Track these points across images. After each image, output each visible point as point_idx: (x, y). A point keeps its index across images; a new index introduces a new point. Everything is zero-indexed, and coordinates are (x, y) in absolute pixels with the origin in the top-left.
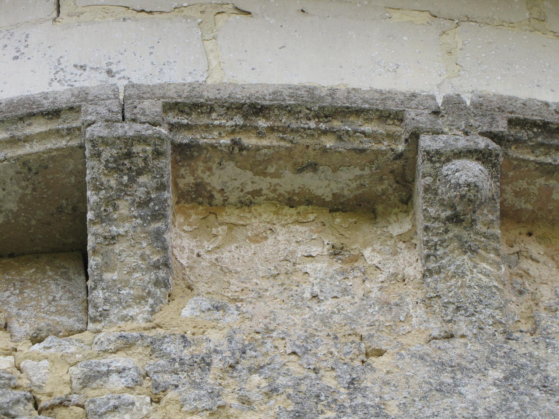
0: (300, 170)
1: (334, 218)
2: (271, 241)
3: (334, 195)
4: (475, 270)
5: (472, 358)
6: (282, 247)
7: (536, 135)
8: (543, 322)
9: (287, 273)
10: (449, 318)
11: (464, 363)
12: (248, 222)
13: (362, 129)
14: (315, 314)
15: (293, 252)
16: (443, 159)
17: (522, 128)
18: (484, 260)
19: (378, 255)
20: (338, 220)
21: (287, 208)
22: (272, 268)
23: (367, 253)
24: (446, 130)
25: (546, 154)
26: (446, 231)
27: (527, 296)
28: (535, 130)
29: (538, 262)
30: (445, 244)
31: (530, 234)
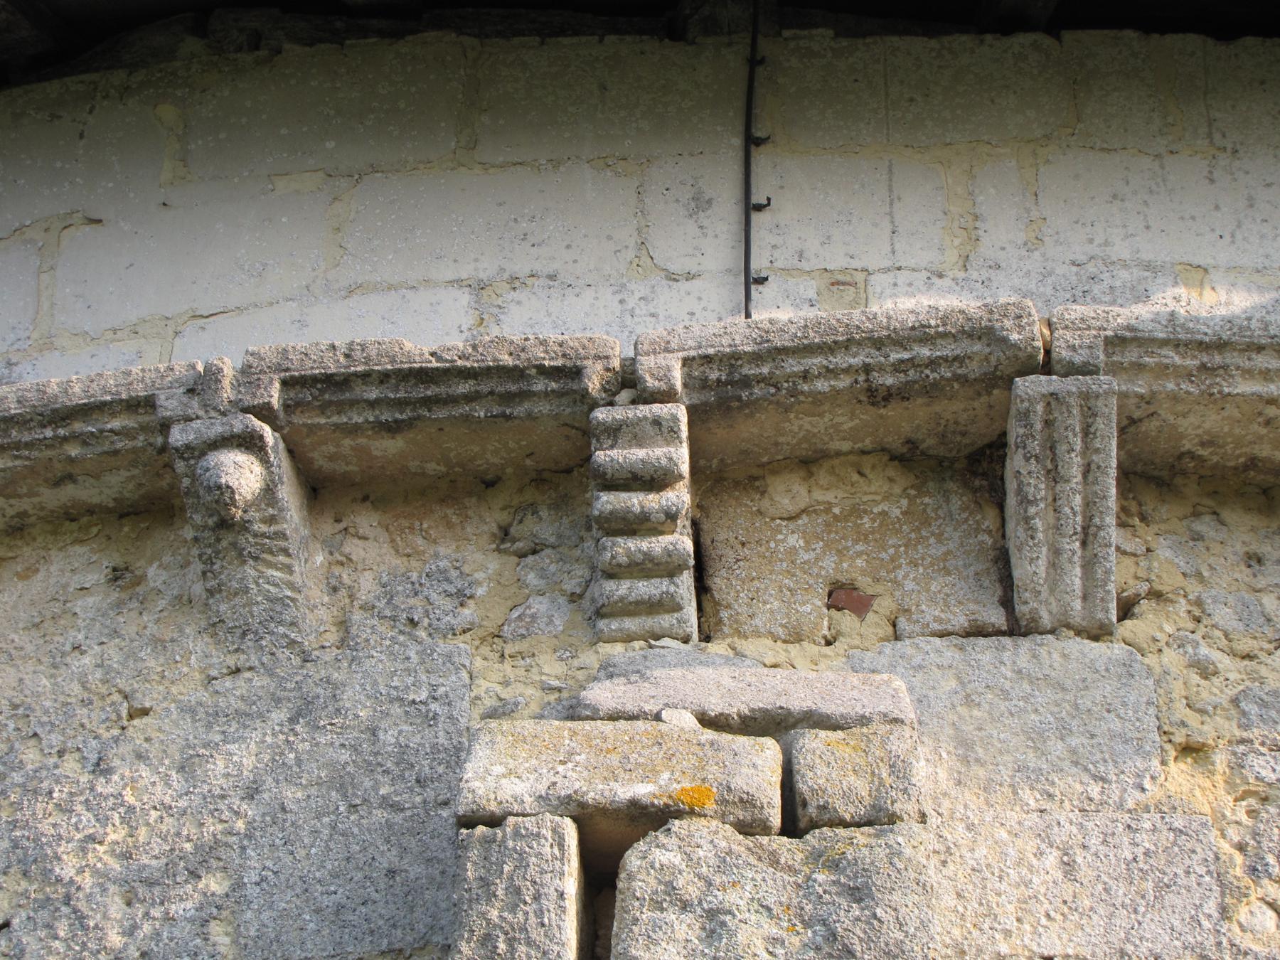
0: (58, 483)
1: (122, 526)
3: (115, 499)
6: (52, 581)
7: (322, 391)
13: (109, 426)
15: (65, 587)
16: (196, 453)
19: (164, 573)
21: (67, 523)
23: (151, 571)
25: (339, 413)
26: (219, 540)
28: (319, 386)
29: (366, 539)
30: (221, 556)
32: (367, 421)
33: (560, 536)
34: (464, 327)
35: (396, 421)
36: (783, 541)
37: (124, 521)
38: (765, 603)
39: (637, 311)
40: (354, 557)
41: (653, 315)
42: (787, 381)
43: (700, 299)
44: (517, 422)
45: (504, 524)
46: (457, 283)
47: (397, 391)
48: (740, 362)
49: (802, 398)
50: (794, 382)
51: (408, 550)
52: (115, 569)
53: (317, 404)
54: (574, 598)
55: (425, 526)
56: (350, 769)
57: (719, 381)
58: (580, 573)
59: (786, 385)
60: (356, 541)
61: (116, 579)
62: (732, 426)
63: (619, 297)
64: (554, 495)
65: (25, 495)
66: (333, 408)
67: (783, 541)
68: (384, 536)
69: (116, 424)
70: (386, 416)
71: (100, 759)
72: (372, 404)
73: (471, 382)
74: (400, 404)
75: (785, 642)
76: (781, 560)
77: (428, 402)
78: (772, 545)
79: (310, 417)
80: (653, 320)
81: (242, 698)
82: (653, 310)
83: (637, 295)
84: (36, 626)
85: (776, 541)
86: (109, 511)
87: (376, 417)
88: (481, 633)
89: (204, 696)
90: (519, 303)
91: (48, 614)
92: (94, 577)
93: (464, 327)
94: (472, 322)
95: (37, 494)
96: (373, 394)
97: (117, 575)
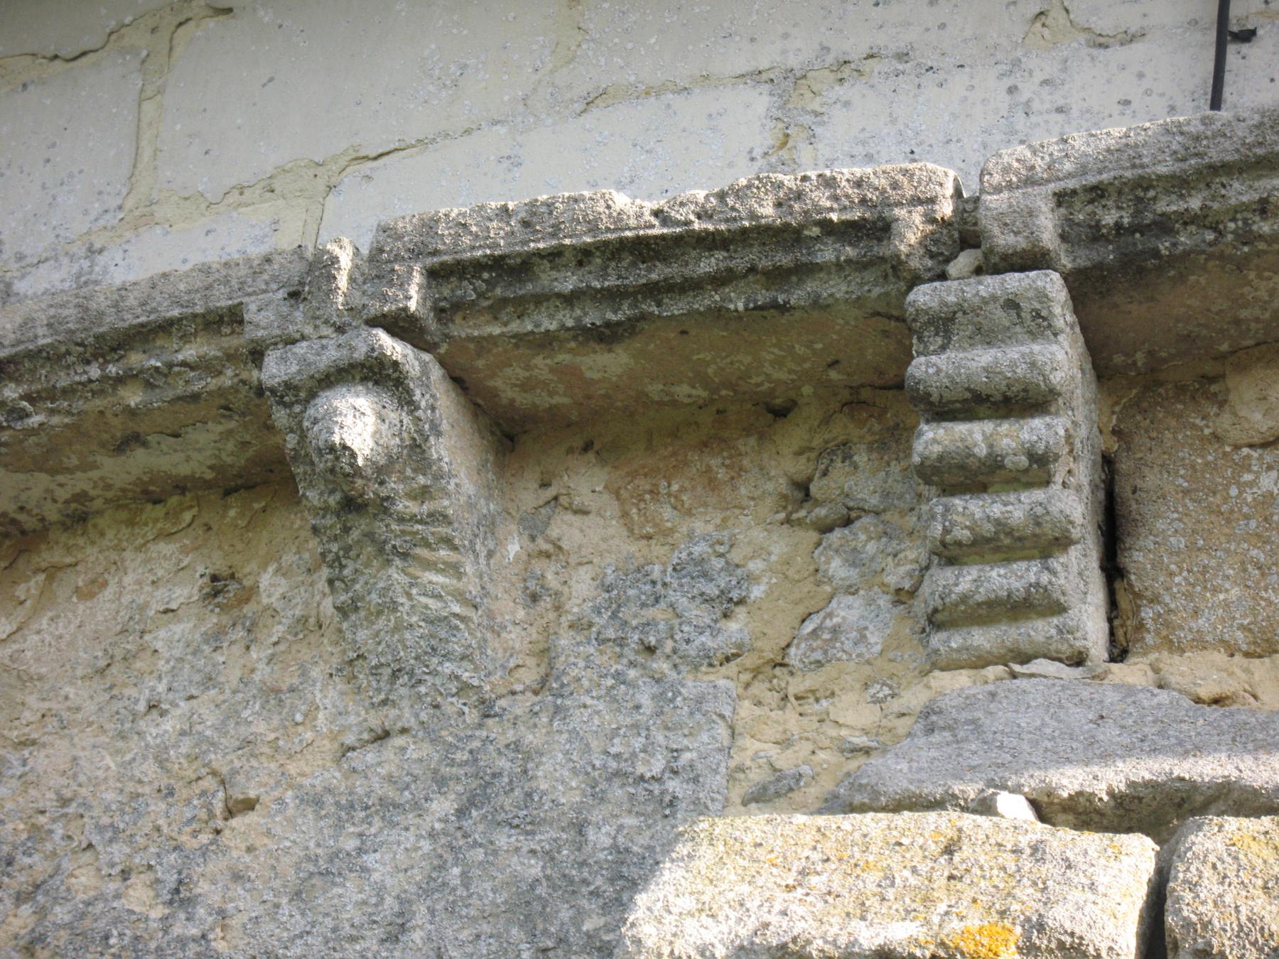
1: (226, 508)
2: (109, 593)
4: (414, 591)
5: (408, 779)
6: (126, 600)
7: (491, 284)
8: (563, 658)
9: (125, 659)
10: (382, 696)
11: (392, 794)
12: (80, 556)
13: (180, 357)
14: (147, 746)
16: (303, 395)
17: (461, 278)
18: (429, 565)
19: (283, 581)
20: (232, 513)
21: (149, 506)
22: (100, 654)
24: (308, 330)
26: (346, 530)
27: (546, 602)
28: (486, 275)
29: (583, 512)
31: (587, 447)
32: (563, 327)
33: (886, 495)
34: (758, 152)
35: (608, 324)
36: (1251, 484)
37: (231, 500)
38: (1216, 590)
39: (1036, 105)
40: (565, 544)
41: (1060, 110)
42: (1234, 220)
43: (1141, 75)
44: (798, 314)
45: (800, 477)
46: (755, 76)
47: (605, 276)
48: (1151, 193)
49: (1262, 246)
50: (1245, 221)
51: (649, 529)
52: (214, 578)
53: (486, 303)
54: (902, 596)
55: (675, 487)
56: (541, 891)
57: (1118, 226)
58: (911, 555)
59: (1232, 225)
60: (569, 517)
61: (216, 593)
62: (1152, 299)
63: (1008, 82)
64: (877, 427)
65: (77, 468)
66: (510, 309)
67: (1251, 484)
68: (612, 508)
69: (190, 352)
70: (593, 316)
71: (180, 882)
72: (570, 299)
73: (720, 255)
74: (612, 296)
75: (1247, 655)
76: (1247, 517)
77: (654, 291)
78: (1234, 491)
79: (476, 326)
80: (1060, 117)
81: (390, 779)
82: (1061, 102)
83: (1038, 77)
84: (102, 672)
85: (1238, 484)
86: (208, 485)
87: (578, 320)
88: (749, 660)
89: (335, 777)
90: (847, 104)
91: (119, 653)
92: (185, 592)
93: (758, 152)
94: (771, 142)
95: (94, 466)
96: (569, 282)
97: (217, 586)
